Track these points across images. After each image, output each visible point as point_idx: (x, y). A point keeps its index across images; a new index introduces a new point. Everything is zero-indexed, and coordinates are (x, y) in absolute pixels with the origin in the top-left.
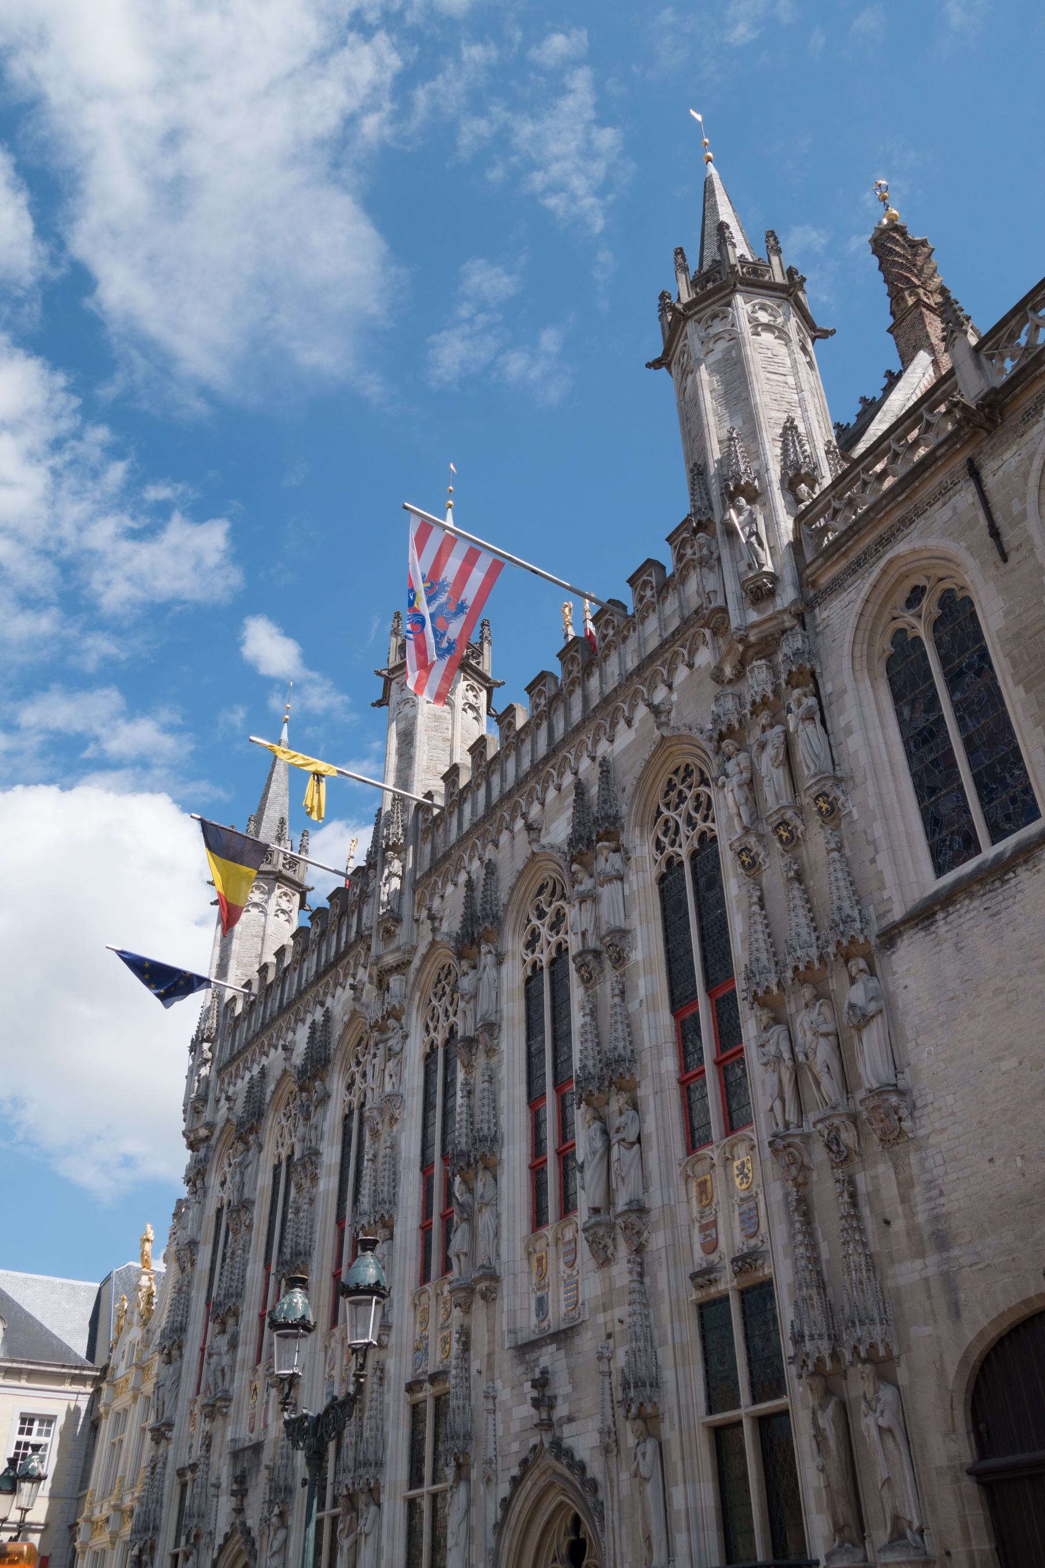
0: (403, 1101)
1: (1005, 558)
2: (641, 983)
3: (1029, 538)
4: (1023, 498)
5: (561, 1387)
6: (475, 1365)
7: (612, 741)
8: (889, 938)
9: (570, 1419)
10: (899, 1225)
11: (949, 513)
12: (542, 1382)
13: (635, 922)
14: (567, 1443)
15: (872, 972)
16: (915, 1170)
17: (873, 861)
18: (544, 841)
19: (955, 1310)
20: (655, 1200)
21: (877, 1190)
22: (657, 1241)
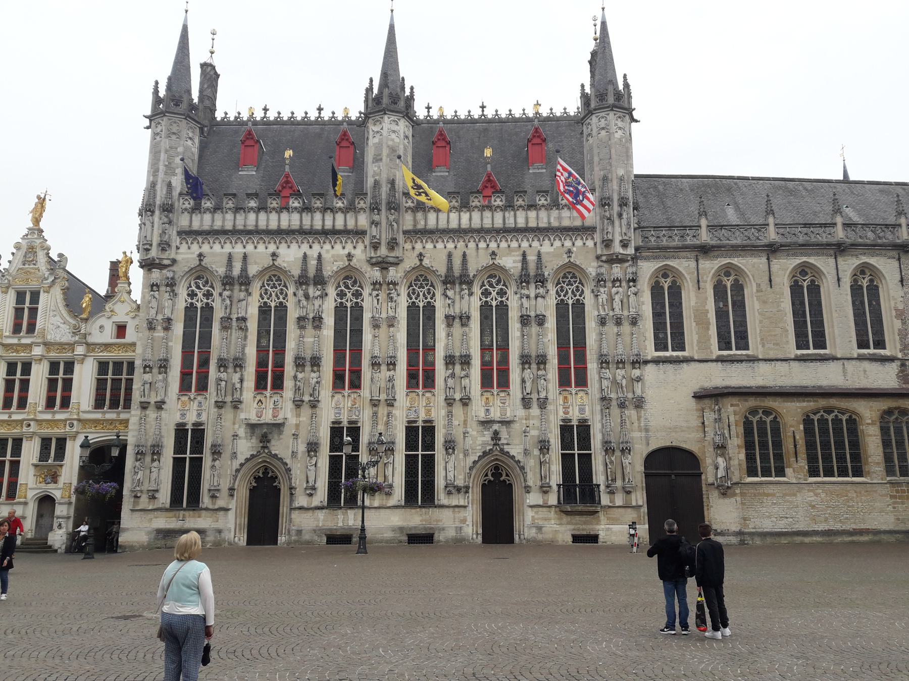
0: (398, 321)
1: (699, 288)
2: (550, 335)
3: (706, 289)
4: (707, 277)
5: (504, 435)
6: (456, 423)
7: (541, 245)
8: (646, 362)
9: (508, 444)
10: (636, 424)
11: (687, 265)
12: (496, 433)
13: (548, 314)
14: (506, 450)
15: (640, 368)
16: (643, 415)
17: (644, 341)
18: (499, 261)
19: (648, 444)
20: (551, 397)
21: (630, 416)
22: (550, 407)
